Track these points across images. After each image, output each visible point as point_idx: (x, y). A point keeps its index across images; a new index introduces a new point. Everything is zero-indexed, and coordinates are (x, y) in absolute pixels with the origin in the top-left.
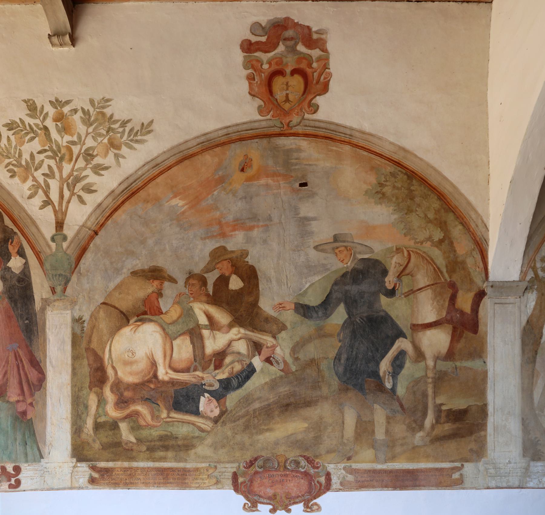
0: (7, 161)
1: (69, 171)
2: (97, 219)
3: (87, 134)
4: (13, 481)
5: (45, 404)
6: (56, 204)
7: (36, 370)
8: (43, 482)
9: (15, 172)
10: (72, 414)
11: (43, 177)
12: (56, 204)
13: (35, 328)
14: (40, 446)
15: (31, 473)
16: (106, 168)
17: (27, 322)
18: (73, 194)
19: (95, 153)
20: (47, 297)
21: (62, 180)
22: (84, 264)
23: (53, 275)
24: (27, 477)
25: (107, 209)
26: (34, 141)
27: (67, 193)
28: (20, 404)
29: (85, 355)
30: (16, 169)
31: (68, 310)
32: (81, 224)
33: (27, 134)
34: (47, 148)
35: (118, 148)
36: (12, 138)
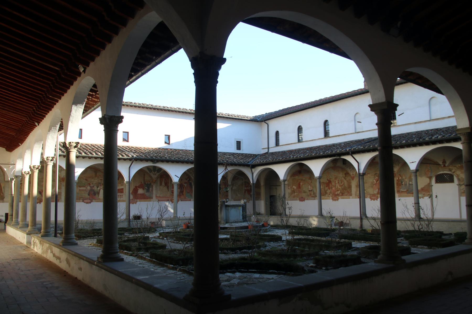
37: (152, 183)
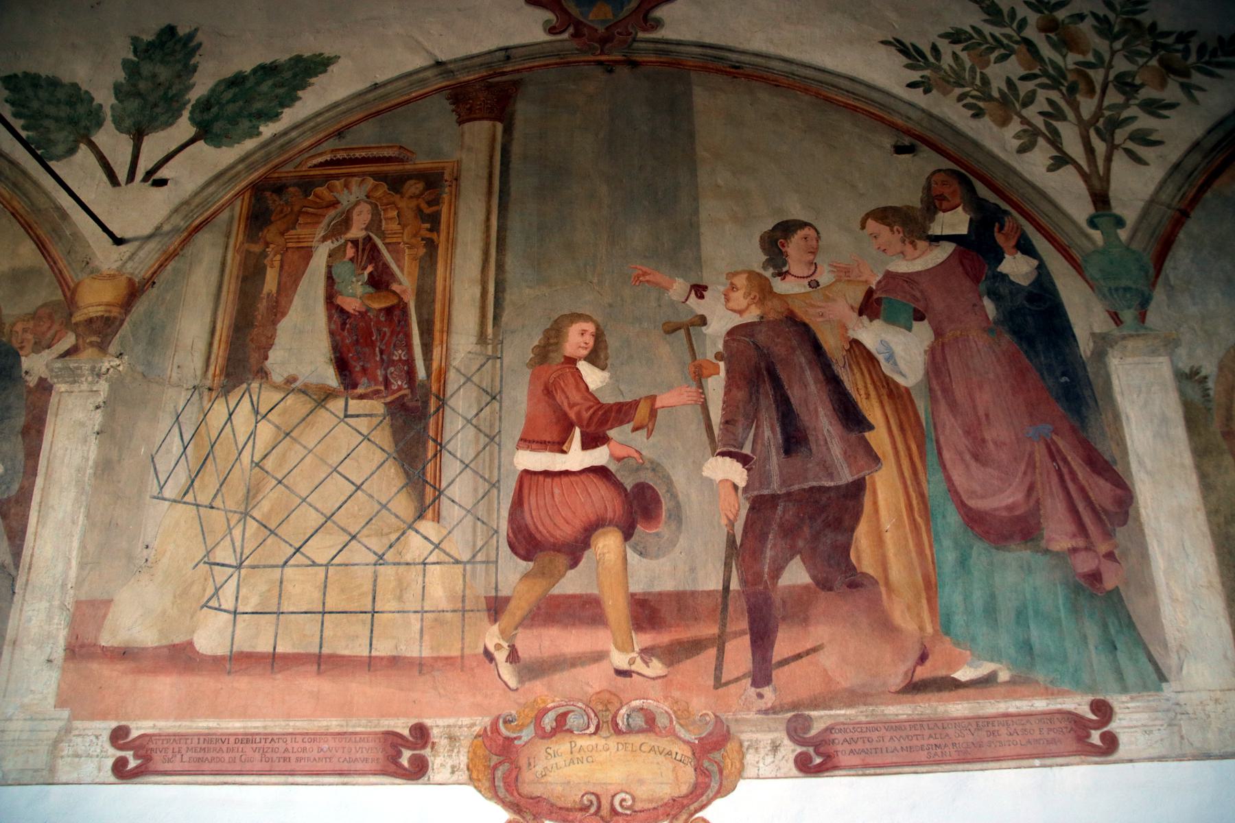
0: (958, 91)
1: (1093, 108)
2: (1179, 190)
3: (1113, 53)
4: (1095, 737)
5: (1144, 556)
6: (1083, 163)
7: (1106, 480)
8: (1177, 739)
9: (980, 108)
10: (1222, 576)
11: (1041, 118)
12: (1083, 163)
13: (1087, 393)
14: (1153, 652)
15: (1143, 717)
16: (1171, 106)
17: (1064, 379)
18: (1112, 148)
19: (1138, 81)
20: (1105, 329)
21: (1084, 127)
22: (1175, 268)
23: (1110, 289)
24: (1132, 727)
25: (1196, 173)
26: (1009, 61)
27: (1100, 147)
28: (1081, 556)
29: (1225, 446)
30: (981, 104)
31: (1160, 355)
32: (1147, 197)
33: (992, 50)
34: (1037, 71)
35: (1187, 74)
36: (964, 55)
37: (39, 347)
